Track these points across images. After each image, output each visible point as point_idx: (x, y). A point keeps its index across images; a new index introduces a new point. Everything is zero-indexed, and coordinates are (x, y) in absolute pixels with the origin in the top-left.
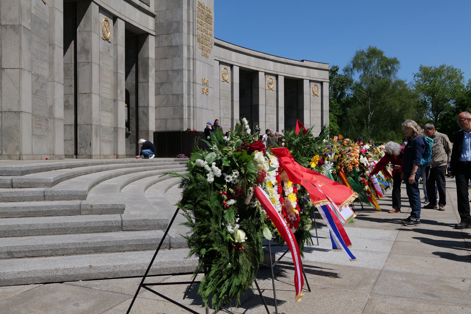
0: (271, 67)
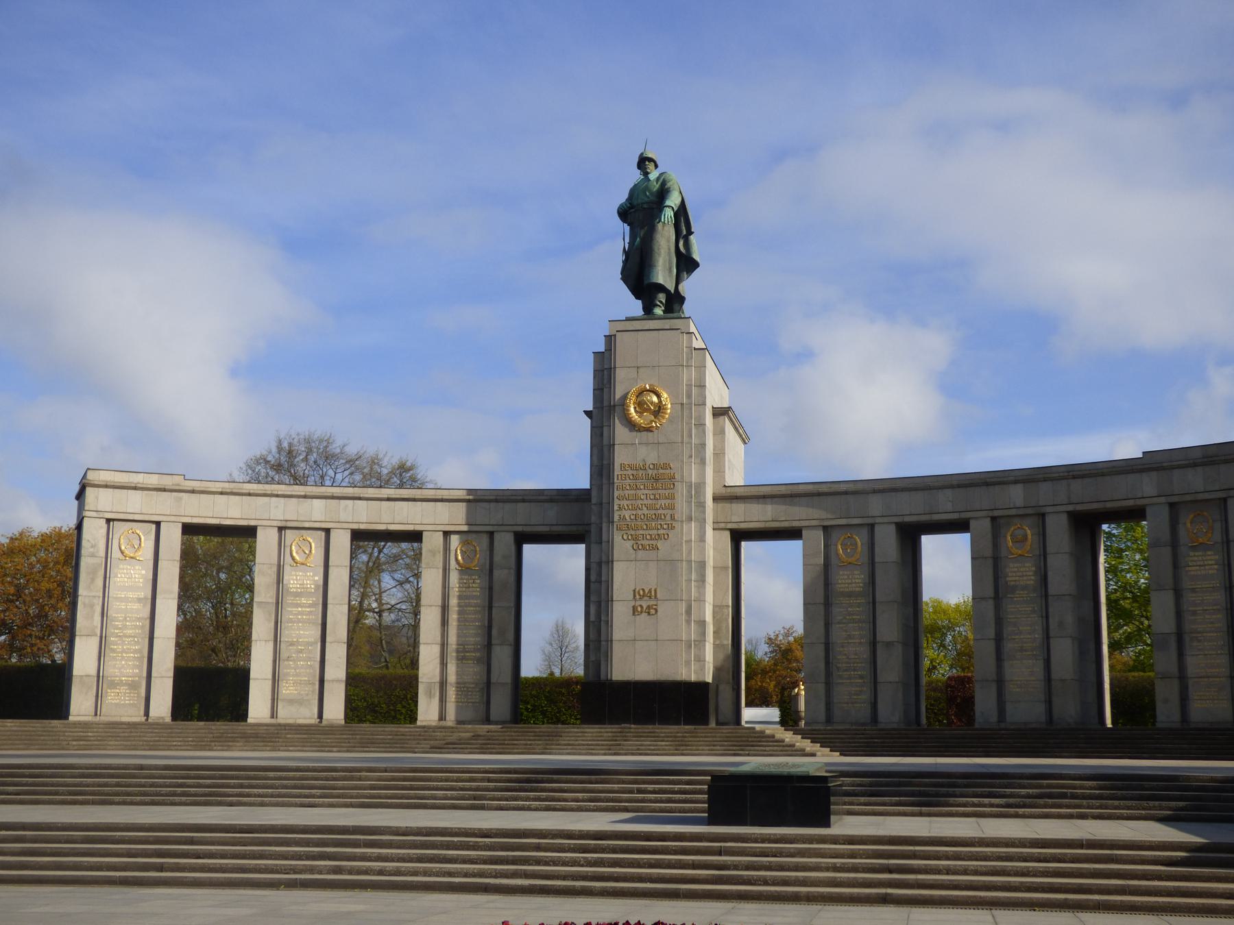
0: (1017, 495)
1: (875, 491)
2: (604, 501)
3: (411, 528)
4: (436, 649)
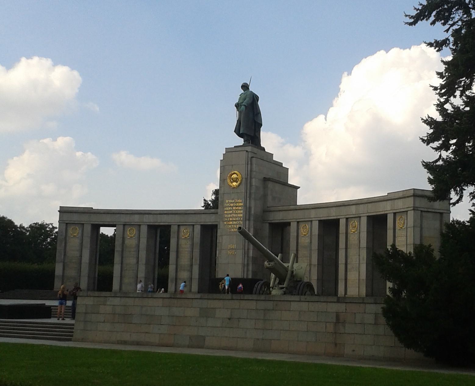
0: (353, 210)
3: (167, 224)
4: (175, 266)
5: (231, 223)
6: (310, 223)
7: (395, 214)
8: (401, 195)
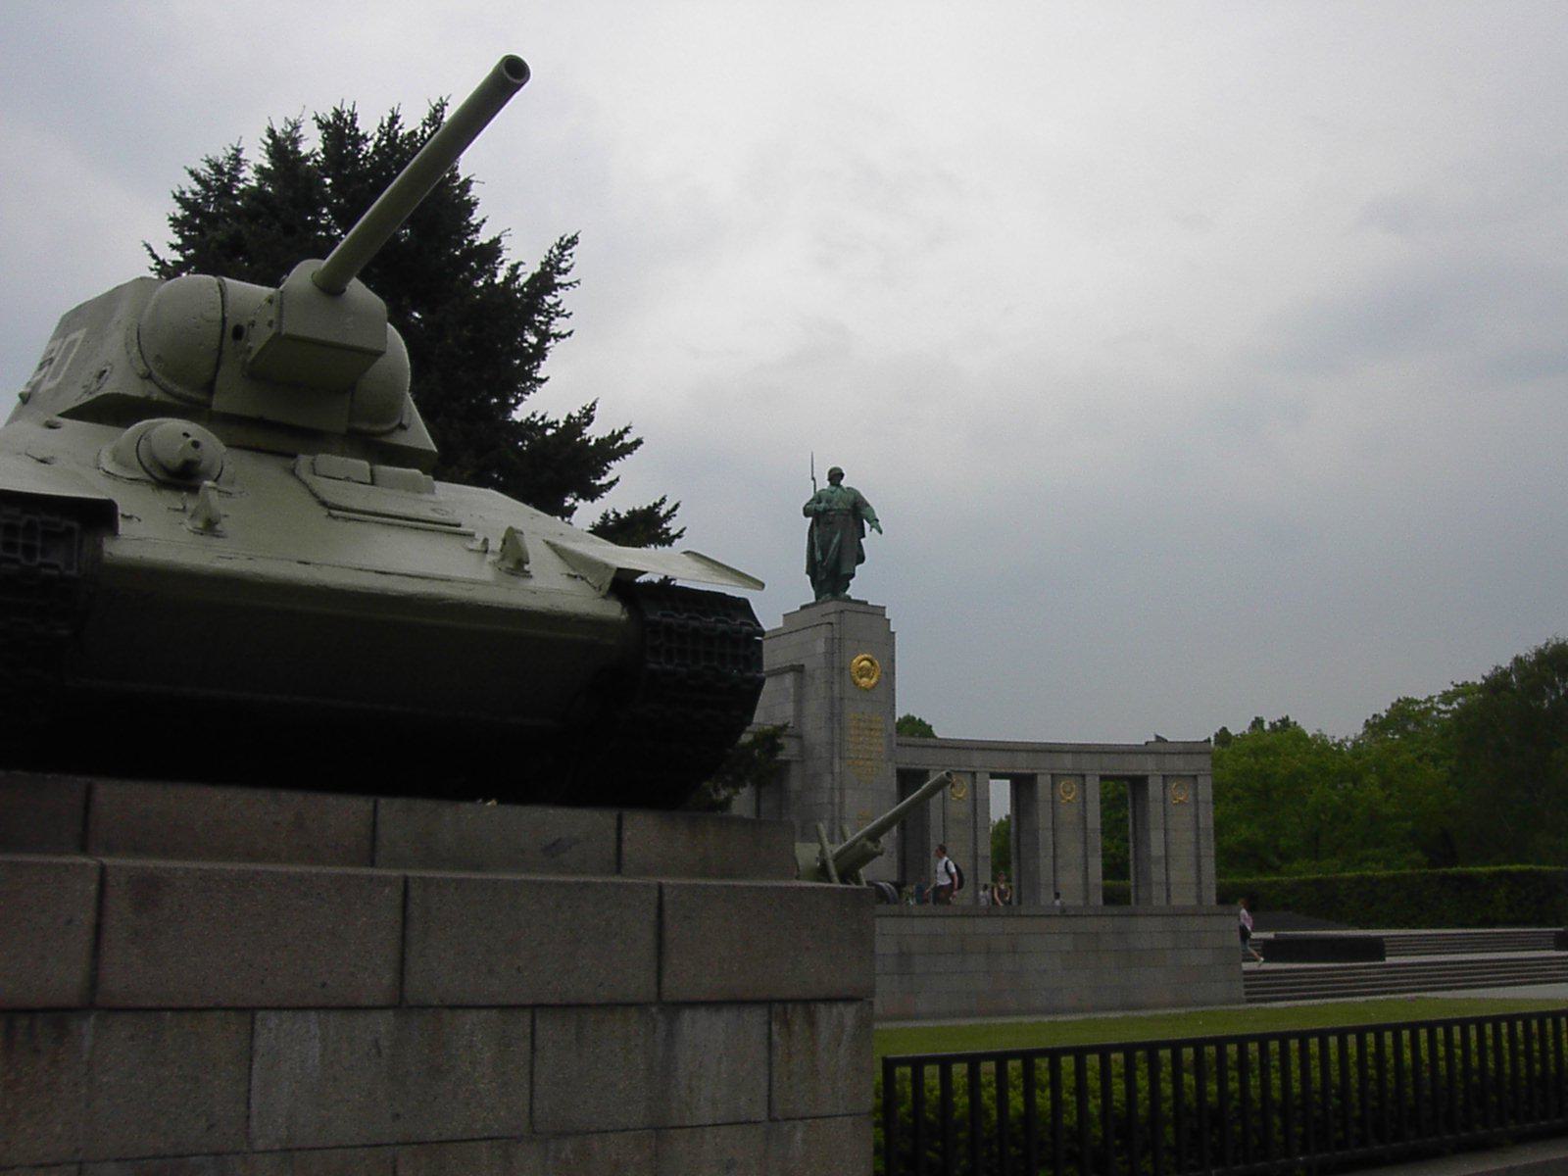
0: (1068, 761)
1: (977, 749)
2: (836, 740)
5: (861, 763)
6: (969, 775)
7: (1164, 776)
8: (1181, 748)
